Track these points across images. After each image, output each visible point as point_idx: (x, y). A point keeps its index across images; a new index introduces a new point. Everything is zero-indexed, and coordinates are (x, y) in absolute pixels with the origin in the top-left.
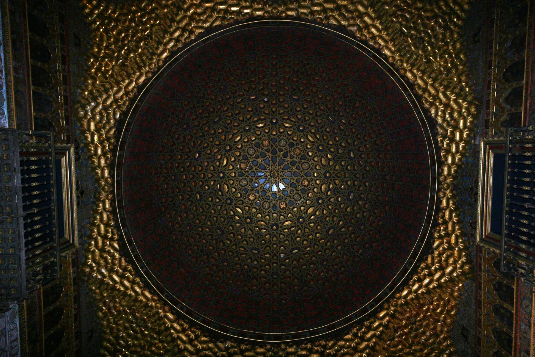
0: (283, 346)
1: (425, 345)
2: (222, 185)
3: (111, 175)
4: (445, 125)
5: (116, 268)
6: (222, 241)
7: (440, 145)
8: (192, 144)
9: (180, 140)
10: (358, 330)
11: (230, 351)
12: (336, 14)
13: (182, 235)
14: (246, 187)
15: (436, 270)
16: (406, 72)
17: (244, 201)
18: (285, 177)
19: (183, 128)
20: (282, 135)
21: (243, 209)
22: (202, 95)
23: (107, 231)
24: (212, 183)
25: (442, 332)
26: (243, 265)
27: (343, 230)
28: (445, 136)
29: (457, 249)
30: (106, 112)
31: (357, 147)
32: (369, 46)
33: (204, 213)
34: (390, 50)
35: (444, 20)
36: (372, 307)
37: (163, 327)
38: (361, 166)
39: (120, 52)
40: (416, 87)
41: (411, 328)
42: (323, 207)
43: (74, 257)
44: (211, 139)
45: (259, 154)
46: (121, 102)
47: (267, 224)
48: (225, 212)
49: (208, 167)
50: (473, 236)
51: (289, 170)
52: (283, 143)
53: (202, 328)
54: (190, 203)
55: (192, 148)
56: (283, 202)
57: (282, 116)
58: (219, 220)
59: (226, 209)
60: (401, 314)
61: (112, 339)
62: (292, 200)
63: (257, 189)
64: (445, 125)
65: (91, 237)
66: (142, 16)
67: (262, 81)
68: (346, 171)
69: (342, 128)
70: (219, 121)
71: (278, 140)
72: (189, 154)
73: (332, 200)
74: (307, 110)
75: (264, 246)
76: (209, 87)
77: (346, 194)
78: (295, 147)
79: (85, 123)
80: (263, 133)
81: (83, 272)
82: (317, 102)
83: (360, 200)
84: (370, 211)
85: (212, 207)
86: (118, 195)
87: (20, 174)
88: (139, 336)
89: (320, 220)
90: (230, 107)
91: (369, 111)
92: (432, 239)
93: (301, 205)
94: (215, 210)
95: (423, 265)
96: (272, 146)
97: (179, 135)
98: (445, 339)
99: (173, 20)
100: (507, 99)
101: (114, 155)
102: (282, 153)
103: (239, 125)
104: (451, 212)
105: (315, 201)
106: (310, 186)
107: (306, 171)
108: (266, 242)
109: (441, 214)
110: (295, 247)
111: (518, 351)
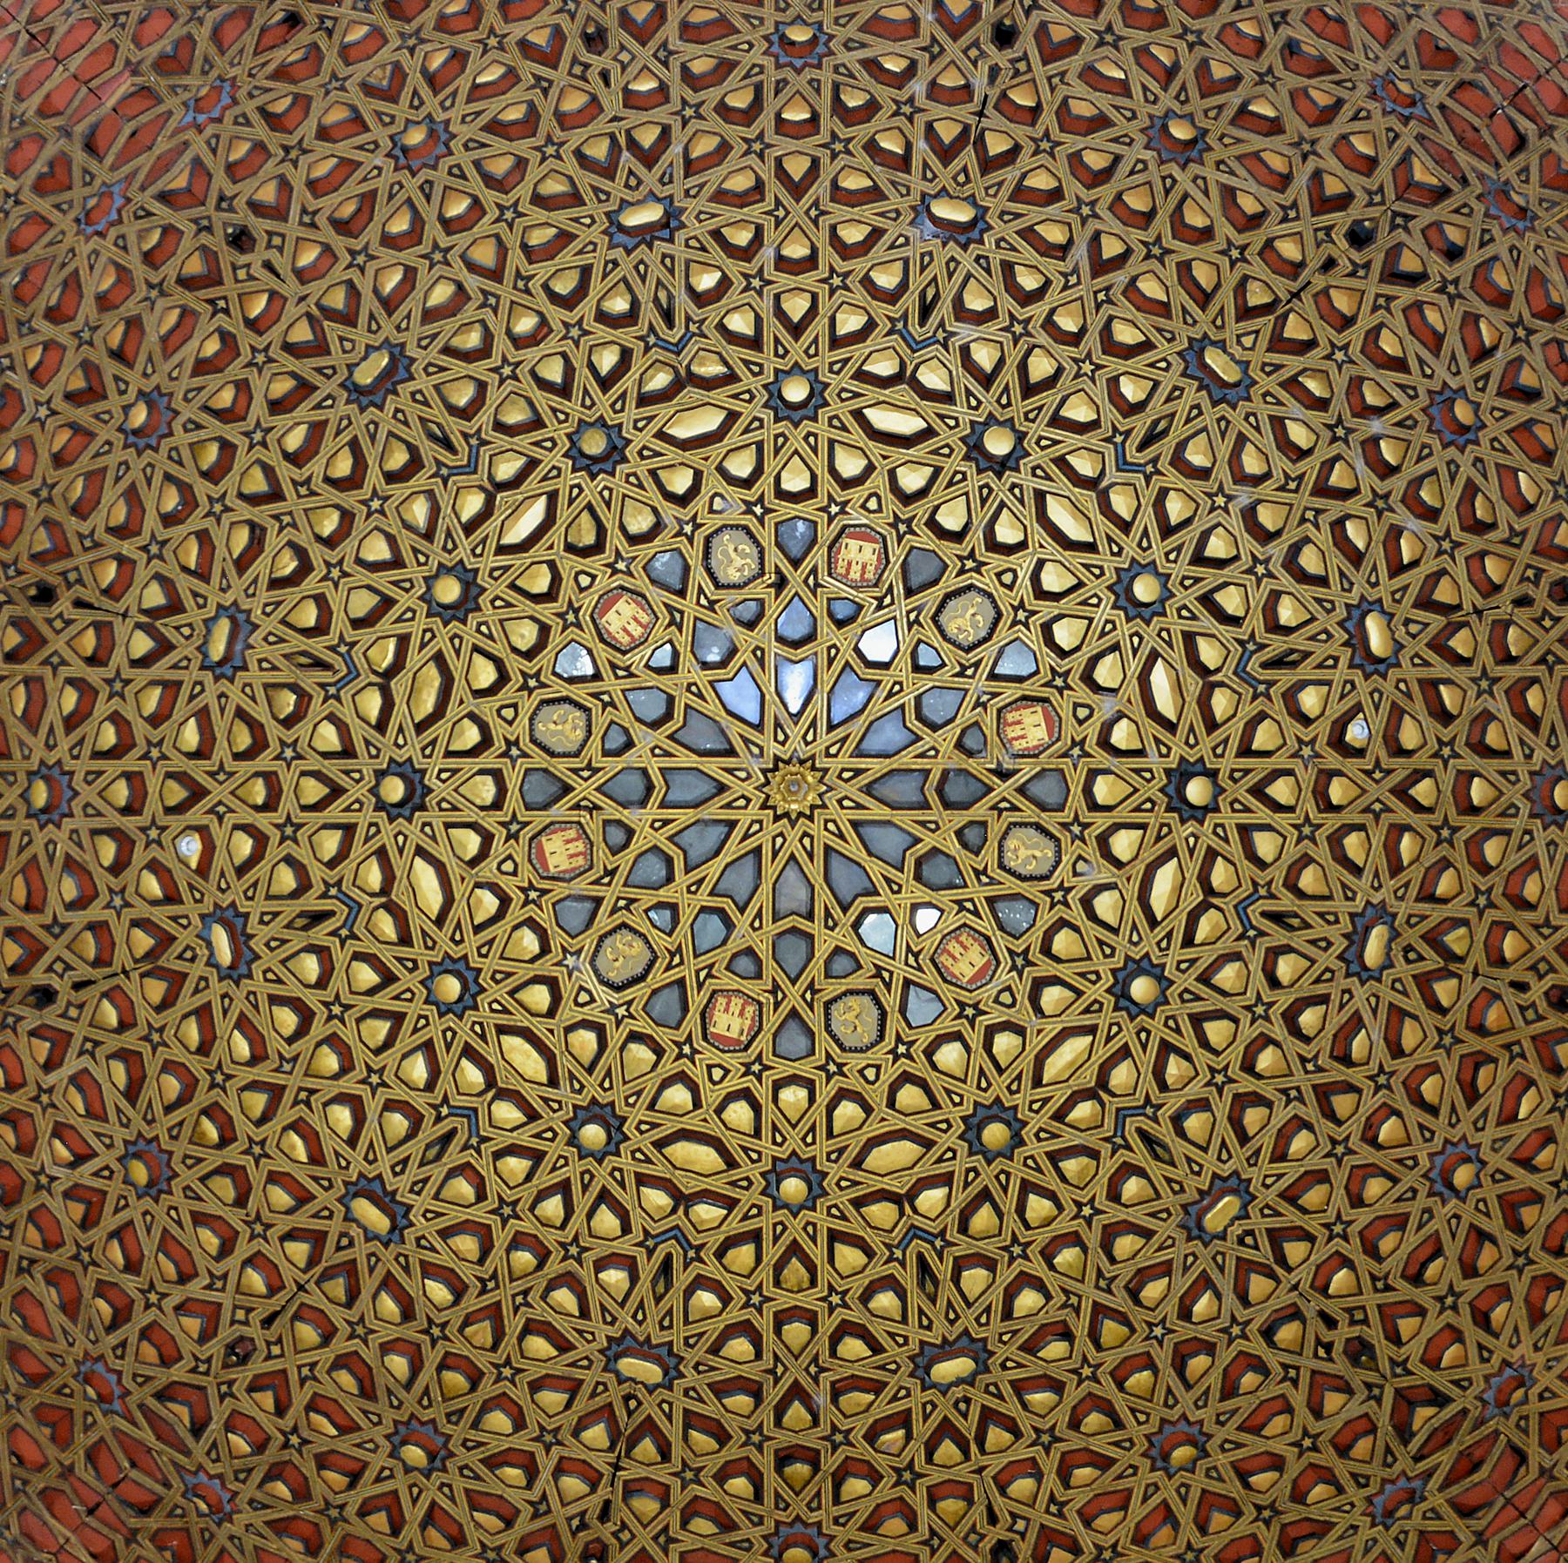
2: (720, 395)
6: (304, 388)
8: (1041, 181)
13: (368, 90)
14: (699, 576)
17: (595, 563)
18: (770, 871)
19: (1169, 114)
20: (1091, 851)
21: (539, 551)
22: (1409, 263)
24: (740, 323)
26: (127, 548)
27: (388, 1305)
31: (1011, 1408)
33: (516, 258)
38: (871, 1436)
42: (554, 1150)
44: (1068, 324)
48: (515, 416)
49: (860, 295)
51: (824, 897)
52: (1027, 852)
54: (599, 151)
55: (1010, 175)
57: (1235, 849)
58: (458, 367)
59: (537, 423)
63: (686, 660)
67: (1500, 706)
68: (827, 1325)
69: (1153, 1290)
70: (1209, 381)
71: (1047, 819)
72: (968, 157)
73: (607, 1220)
74: (1278, 1031)
75: (260, 713)
76: (1471, 320)
78: (1000, 942)
80: (1106, 707)
82: (1342, 1104)
83: (614, 1435)
84: (540, 1507)
85: (556, 315)
90: (1311, 467)
93: (567, 988)
94: (533, 340)
96: (1004, 775)
97: (1124, 88)
102: (953, 847)
103: (1167, 530)
105: (592, 1090)
106: (709, 1055)
107: (815, 1020)
108: (288, 722)
110: (257, 945)
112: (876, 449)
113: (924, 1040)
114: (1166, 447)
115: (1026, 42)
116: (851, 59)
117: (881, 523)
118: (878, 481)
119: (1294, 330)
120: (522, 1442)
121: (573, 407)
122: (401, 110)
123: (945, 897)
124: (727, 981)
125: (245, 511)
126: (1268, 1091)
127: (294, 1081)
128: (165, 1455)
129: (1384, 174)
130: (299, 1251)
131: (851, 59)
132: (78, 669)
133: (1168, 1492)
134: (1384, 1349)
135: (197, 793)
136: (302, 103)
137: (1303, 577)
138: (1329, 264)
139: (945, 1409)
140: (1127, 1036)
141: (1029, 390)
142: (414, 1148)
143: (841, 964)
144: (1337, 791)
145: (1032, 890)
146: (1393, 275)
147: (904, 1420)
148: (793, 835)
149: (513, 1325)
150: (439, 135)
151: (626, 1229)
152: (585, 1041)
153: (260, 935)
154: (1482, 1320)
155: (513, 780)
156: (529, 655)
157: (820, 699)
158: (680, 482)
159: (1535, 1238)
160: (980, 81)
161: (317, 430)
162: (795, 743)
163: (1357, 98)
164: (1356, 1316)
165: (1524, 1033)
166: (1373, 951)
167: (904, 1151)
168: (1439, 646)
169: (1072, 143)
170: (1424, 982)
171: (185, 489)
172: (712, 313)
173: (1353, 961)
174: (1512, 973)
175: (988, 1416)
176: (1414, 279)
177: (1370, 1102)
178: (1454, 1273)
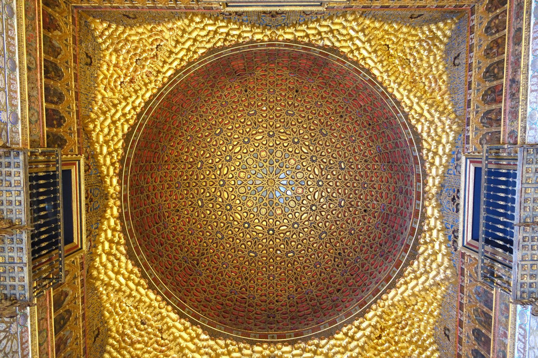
0: (266, 39)
1: (127, 40)
3: (424, 207)
6: (322, 123)
7: (121, 235)
8: (346, 214)
10: (193, 57)
11: (320, 37)
15: (119, 119)
22: (336, 260)
24: (329, 177)
25: (111, 54)
27: (207, 134)
28: (118, 243)
29: (101, 143)
32: (190, 321)
34: (171, 318)
35: (124, 341)
36: (179, 77)
37: (385, 63)
39: (410, 317)
40: (146, 286)
41: (140, 56)
42: (226, 153)
43: (467, 146)
46: (412, 276)
48: (318, 149)
50: (87, 158)
52: (263, 211)
53: (346, 58)
60: (151, 73)
61: (435, 50)
64: (118, 255)
65: (449, 156)
66: (389, 347)
67: (282, 270)
68: (205, 188)
69: (210, 227)
70: (322, 234)
73: (217, 160)
75: (281, 117)
76: (330, 268)
79: (446, 263)
80: (281, 221)
81: (459, 126)
85: (330, 154)
86: (419, 187)
87: (514, 260)
88: (408, 51)
89: (228, 141)
90: (311, 247)
91: (185, 247)
92: (125, 149)
95: (132, 122)
98: (107, 48)
100: (67, 295)
101: (421, 226)
104: (108, 175)
107: (242, 185)
109: (117, 171)
111: (39, 66)
115: (364, 214)
118: (309, 193)
119: (328, 245)
120: (190, 151)
121: (319, 156)
122: (357, 137)
127: (235, 121)
128: (189, 108)
130: (214, 123)
132: (287, 95)
133: (186, 231)
136: (359, 125)
139: (195, 202)
141: (320, 212)
144: (271, 250)
146: (335, 258)
147: (193, 198)
149: (205, 149)
150: (354, 141)
152: (239, 157)
153: (253, 117)
154: (207, 269)
155: (272, 148)
158: (309, 169)
161: (317, 125)
165: (242, 274)
166: (251, 254)
167: (226, 196)
168: (289, 262)
169: (351, 219)
170: (248, 261)
171: (310, 108)
173: (250, 252)
175: (194, 208)
177: (233, 254)
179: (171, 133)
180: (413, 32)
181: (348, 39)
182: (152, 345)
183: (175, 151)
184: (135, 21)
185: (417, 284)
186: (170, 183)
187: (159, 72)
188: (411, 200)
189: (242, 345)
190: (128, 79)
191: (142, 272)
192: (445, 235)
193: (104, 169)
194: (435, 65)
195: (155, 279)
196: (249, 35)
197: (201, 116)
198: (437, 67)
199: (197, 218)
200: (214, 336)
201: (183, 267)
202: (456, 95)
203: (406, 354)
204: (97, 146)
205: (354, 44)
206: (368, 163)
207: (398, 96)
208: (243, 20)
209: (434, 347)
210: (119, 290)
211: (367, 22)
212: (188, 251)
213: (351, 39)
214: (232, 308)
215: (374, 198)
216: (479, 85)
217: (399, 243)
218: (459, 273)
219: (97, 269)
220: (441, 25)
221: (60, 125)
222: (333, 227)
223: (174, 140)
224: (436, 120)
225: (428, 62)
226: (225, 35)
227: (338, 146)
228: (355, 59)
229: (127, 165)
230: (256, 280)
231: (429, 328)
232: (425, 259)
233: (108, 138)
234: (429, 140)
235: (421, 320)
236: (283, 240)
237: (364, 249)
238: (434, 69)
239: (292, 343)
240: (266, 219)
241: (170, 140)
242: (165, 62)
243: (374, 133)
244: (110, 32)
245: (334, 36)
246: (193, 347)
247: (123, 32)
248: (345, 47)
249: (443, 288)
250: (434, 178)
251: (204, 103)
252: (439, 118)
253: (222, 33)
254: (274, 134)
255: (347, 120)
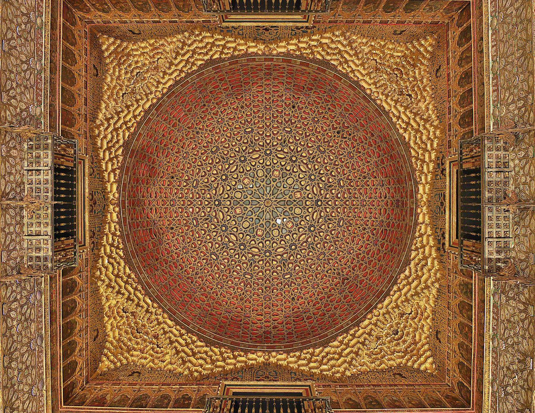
0: (117, 209)
1: (119, 341)
3: (278, 54)
4: (323, 354)
5: (196, 56)
7: (305, 351)
8: (299, 126)
9: (303, 114)
10: (133, 279)
11: (115, 159)
12: (421, 256)
14: (256, 175)
15: (191, 349)
16: (369, 319)
17: (243, 174)
18: (265, 213)
20: (306, 211)
21: (236, 172)
22: (345, 136)
23: (229, 48)
25: (132, 356)
27: (216, 268)
28: (312, 354)
30: (338, 53)
32: (392, 286)
33: (233, 135)
34: (389, 304)
35: (412, 351)
37: (139, 97)
39: (389, 66)
40: (357, 328)
42: (237, 249)
45: (287, 188)
46: (345, 66)
47: (220, 195)
49: (276, 140)
50: (226, 379)
51: (272, 217)
52: (298, 211)
56: (242, 211)
60: (148, 319)
62: (243, 220)
63: (254, 186)
64: (323, 354)
67: (357, 192)
68: (272, 271)
69: (313, 267)
70: (320, 151)
72: (289, 123)
75: (200, 193)
77: (249, 271)
80: (308, 192)
81: (195, 28)
82: (337, 243)
88: (129, 75)
92: (220, 346)
96: (295, 201)
98: (127, 359)
99: (416, 114)
100: (350, 399)
101: (297, 57)
106: (257, 237)
107: (271, 233)
108: (203, 194)
109: (242, 354)
112: (278, 159)
113: (284, 235)
114: (315, 159)
115: (296, 108)
116: (274, 110)
117: (279, 169)
118: (279, 164)
121: (240, 154)
122: (218, 117)
123: (287, 217)
124: (259, 228)
125: (198, 167)
126: (328, 241)
129: (341, 125)
130: (205, 261)
131: (274, 110)
132: (177, 187)
134: (341, 273)
135: (192, 203)
136: (205, 116)
137: (333, 176)
138: (335, 136)
140: (310, 234)
141: (298, 152)
142: (219, 249)
143: (274, 226)
145: (298, 216)
146: (342, 137)
148: (268, 209)
149: (232, 271)
151: (246, 259)
154: (353, 269)
156: (234, 186)
157: (271, 192)
159: (360, 259)
160: (291, 113)
162: (268, 197)
163: (337, 115)
164: (338, 269)
169: (303, 121)
172: (257, 142)
174: (358, 226)
176: (345, 138)
178: (350, 263)
179: (213, 303)
180: (111, 71)
181: (117, 133)
182: (416, 324)
183: (232, 300)
184: (100, 331)
185: (352, 61)
186: (264, 305)
187: (147, 311)
188: (275, 65)
189: (417, 234)
190: (155, 341)
191: (342, 333)
192: (303, 36)
193: (239, 365)
194: (141, 50)
195: (352, 321)
196: (113, 225)
197: (196, 274)
198: (143, 48)
199: (302, 279)
200: (408, 262)
201: (348, 293)
202: (167, 31)
203: (425, 70)
204: (216, 370)
205: (121, 127)
206: (244, 105)
207: (171, 83)
208: (99, 231)
209: (416, 43)
210: (357, 353)
211: (101, 116)
212: (334, 289)
213: (116, 130)
214: (389, 244)
215: (279, 99)
216: (154, 15)
217: (319, 76)
218: (335, 25)
219: (334, 373)
220: (104, 47)
221: (190, 399)
222: (313, 139)
223: (220, 301)
224: (192, 48)
225: (140, 56)
226: (113, 248)
227: (229, 135)
228: (135, 125)
229: (239, 345)
230: (365, 219)
231: (399, 48)
232: (328, 54)
233: (208, 360)
234: (211, 53)
235: (392, 56)
236: (327, 190)
237: (332, 108)
238: (145, 51)
239: (417, 183)
240: (305, 208)
241: (220, 305)
242: (138, 305)
243: (213, 101)
244: (110, 355)
245: (114, 146)
246: (416, 283)
247: (112, 343)
248: (123, 136)
249: (354, 37)
250: (249, 47)
251: (183, 270)
252: (189, 46)
253: (110, 250)
254: (217, 200)
255: (201, 127)
